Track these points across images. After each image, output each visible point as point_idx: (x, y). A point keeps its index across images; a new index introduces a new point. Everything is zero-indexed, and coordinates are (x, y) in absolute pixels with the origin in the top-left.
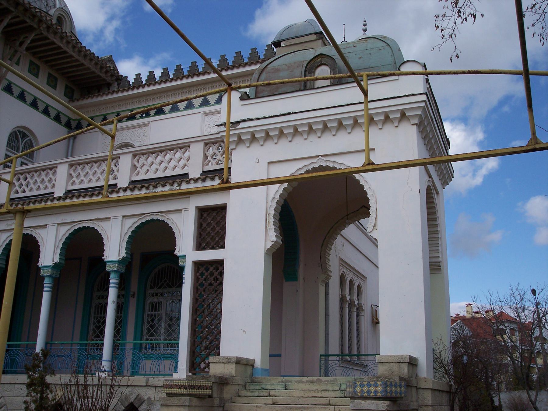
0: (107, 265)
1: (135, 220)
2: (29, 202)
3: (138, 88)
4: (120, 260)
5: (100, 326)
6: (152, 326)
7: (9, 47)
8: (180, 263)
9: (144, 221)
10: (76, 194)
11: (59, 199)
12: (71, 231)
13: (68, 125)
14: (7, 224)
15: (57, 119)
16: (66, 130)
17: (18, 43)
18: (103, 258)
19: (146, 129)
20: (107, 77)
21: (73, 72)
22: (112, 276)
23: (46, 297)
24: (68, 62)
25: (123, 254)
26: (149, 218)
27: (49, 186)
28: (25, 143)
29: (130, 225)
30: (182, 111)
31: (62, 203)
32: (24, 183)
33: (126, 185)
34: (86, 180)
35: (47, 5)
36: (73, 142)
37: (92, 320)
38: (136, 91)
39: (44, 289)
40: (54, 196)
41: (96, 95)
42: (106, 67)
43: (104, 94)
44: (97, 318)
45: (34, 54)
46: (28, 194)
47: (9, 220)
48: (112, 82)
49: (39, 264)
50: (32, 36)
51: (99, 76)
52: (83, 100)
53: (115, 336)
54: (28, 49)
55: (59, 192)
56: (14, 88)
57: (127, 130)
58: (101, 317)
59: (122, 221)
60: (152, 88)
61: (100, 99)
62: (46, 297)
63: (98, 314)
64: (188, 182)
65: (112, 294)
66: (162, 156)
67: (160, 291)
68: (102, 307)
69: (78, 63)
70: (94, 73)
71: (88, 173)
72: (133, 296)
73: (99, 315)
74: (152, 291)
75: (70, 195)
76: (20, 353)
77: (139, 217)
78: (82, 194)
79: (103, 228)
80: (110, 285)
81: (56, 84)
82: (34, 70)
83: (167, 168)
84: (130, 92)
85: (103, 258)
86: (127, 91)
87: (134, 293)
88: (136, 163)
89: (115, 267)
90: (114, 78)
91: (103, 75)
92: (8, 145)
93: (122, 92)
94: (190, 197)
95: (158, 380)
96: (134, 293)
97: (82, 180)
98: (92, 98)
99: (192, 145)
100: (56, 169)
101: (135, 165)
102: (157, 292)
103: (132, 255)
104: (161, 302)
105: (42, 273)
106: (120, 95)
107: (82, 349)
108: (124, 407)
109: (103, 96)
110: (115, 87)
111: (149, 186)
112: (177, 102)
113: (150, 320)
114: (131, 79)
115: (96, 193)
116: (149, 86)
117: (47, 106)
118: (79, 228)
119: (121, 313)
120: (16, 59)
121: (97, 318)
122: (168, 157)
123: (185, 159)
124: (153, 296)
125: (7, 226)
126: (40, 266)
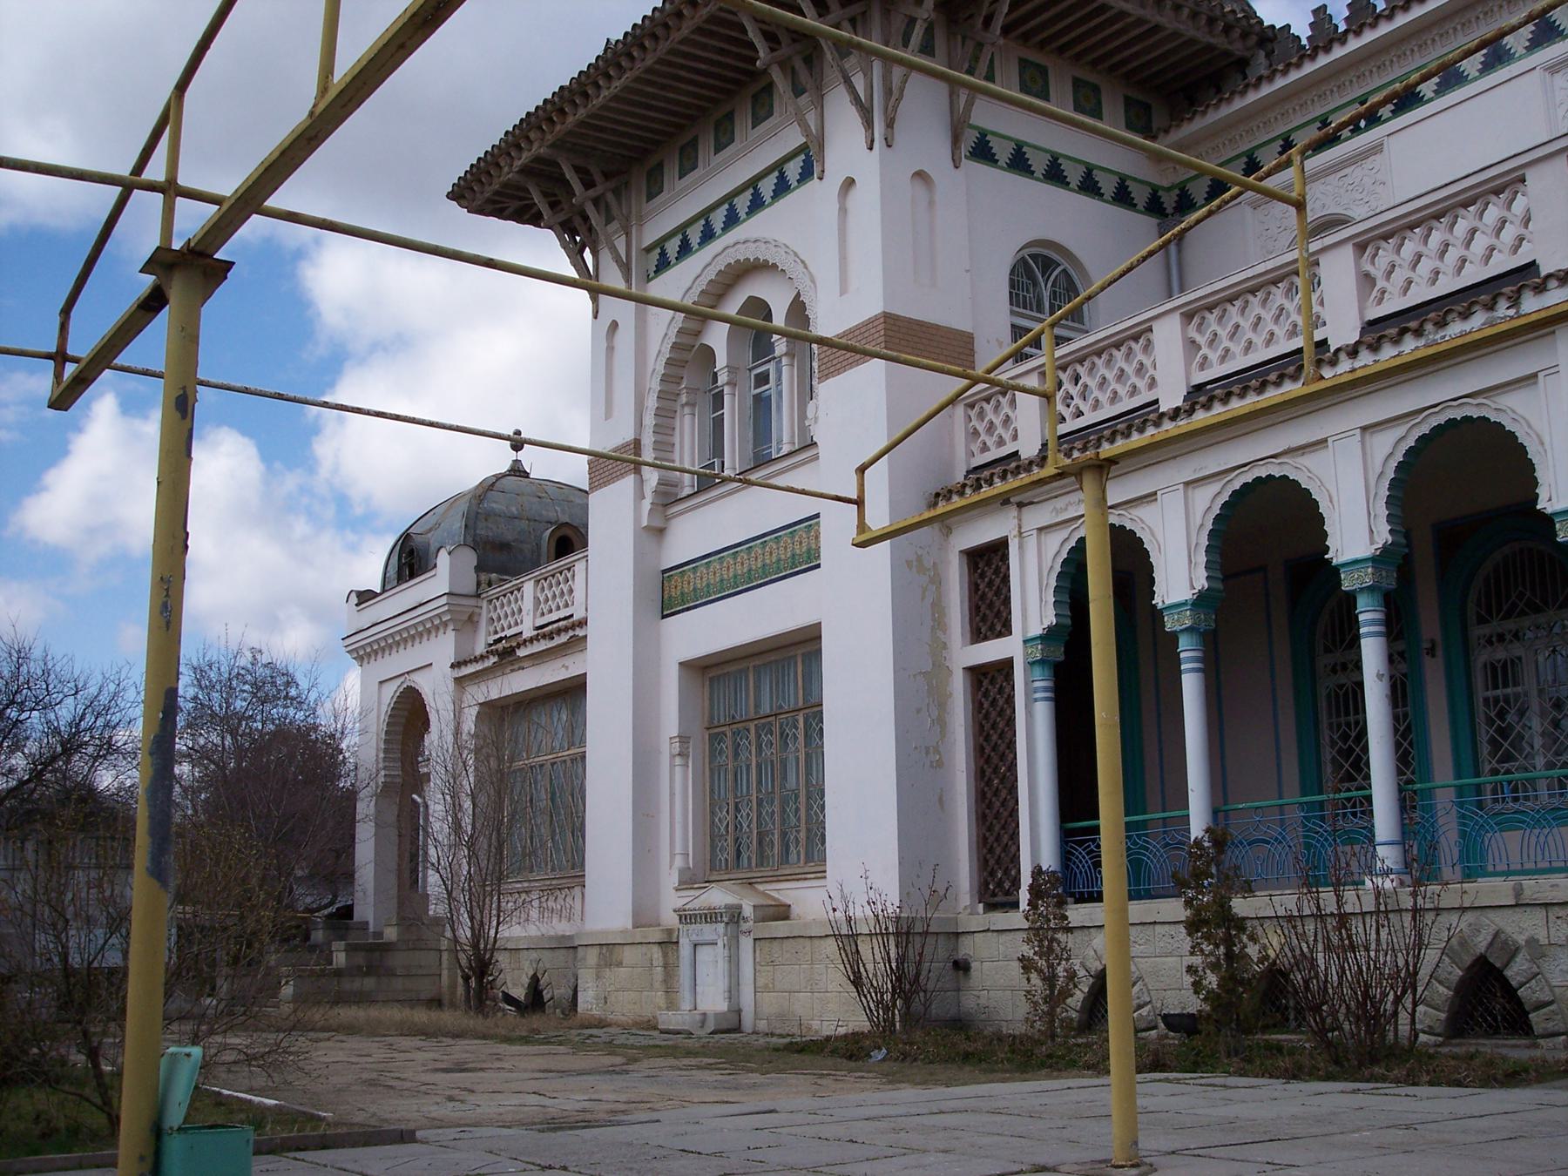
0: (1342, 576)
1: (1400, 431)
2: (1099, 440)
3: (1327, 49)
4: (1378, 553)
5: (1351, 750)
6: (1504, 733)
7: (959, 37)
8: (1561, 534)
9: (1425, 429)
10: (1218, 392)
11: (1175, 414)
12: (1225, 497)
13: (1154, 207)
14: (1055, 508)
15: (1122, 197)
16: (1150, 222)
17: (979, 21)
18: (1326, 556)
19: (1376, 161)
20: (1230, 43)
21: (1137, 55)
22: (1363, 603)
23: (1191, 687)
24: (1119, 33)
25: (1384, 535)
26: (1441, 419)
27: (1141, 384)
29: (1389, 448)
30: (1475, 79)
31: (1184, 425)
32: (1074, 391)
33: (1354, 337)
34: (1236, 348)
36: (1179, 251)
37: (1326, 734)
38: (1323, 60)
39: (1183, 667)
40: (1161, 411)
41: (1214, 102)
42: (1224, 15)
43: (1233, 93)
44: (1339, 726)
45: (1025, 38)
46: (1089, 418)
47: (1056, 497)
48: (1247, 54)
49: (1157, 601)
51: (1210, 48)
52: (1178, 126)
53: (1400, 772)
54: (1006, 30)
55: (1171, 399)
56: (994, 143)
57: (1322, 180)
58: (1348, 725)
59: (1363, 442)
60: (1369, 36)
61: (1225, 111)
62: (1191, 687)
63: (1338, 715)
64: (1540, 289)
65: (1372, 654)
66: (1501, 206)
67: (1511, 625)
68: (1346, 693)
69: (1146, 27)
70: (1191, 42)
71: (1237, 326)
72: (1432, 652)
73: (1342, 719)
74: (1485, 630)
75: (1203, 399)
76: (1151, 844)
77: (1408, 422)
78: (1236, 389)
79: (1308, 472)
80: (1362, 631)
81: (1100, 103)
82: (1035, 81)
83: (1464, 261)
84: (1308, 68)
85: (1326, 556)
86: (1299, 66)
87: (1433, 642)
88: (1368, 267)
89: (1367, 577)
90: (1253, 39)
91: (1219, 41)
92: (1014, 299)
93: (1285, 73)
94: (1554, 332)
95: (1552, 886)
96: (1433, 642)
97: (1227, 351)
98: (1204, 113)
99: (1530, 175)
100: (1149, 334)
101: (1367, 275)
102: (1500, 630)
103: (1407, 536)
104: (1520, 658)
105: (1170, 625)
106: (1280, 82)
107: (1315, 817)
108: (1459, 968)
109: (1233, 99)
110: (1260, 64)
111: (1421, 325)
112: (1503, 34)
113: (1492, 714)
114: (1302, 30)
115: (1273, 377)
116: (1358, 33)
117: (1089, 171)
118: (1245, 485)
119: (1405, 705)
120: (983, 67)
121: (1339, 726)
122: (1462, 227)
123: (1517, 221)
124: (1490, 642)
125: (1054, 514)
126: (1160, 606)
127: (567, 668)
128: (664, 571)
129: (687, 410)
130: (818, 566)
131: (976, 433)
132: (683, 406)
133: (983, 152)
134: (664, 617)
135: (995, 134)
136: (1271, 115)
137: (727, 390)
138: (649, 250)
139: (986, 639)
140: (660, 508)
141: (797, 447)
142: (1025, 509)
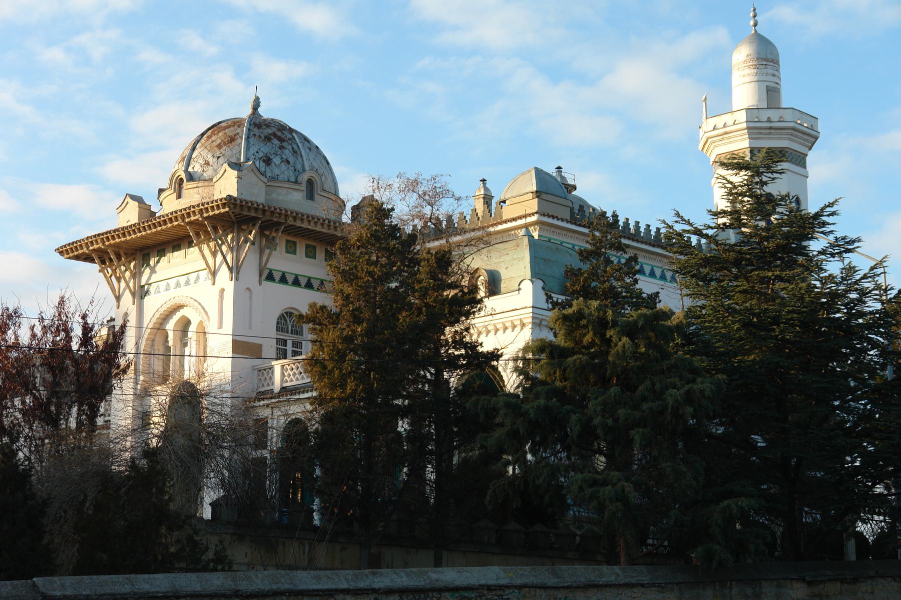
28: (293, 322)
35: (295, 170)
82: (291, 248)
117: (309, 279)
131: (260, 379)
133: (270, 278)
135: (275, 270)
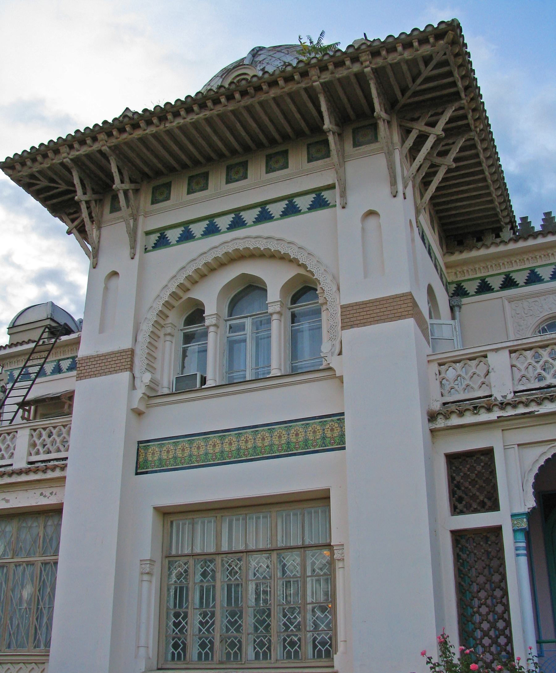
21: (456, 208)
50: (461, 142)
61: (483, 252)
109: (490, 247)
110: (507, 234)
127: (7, 501)
128: (140, 442)
129: (168, 338)
130: (344, 448)
132: (165, 335)
134: (137, 474)
136: (525, 257)
137: (212, 329)
138: (148, 233)
139: (462, 512)
140: (146, 398)
141: (283, 373)
142: (505, 432)
